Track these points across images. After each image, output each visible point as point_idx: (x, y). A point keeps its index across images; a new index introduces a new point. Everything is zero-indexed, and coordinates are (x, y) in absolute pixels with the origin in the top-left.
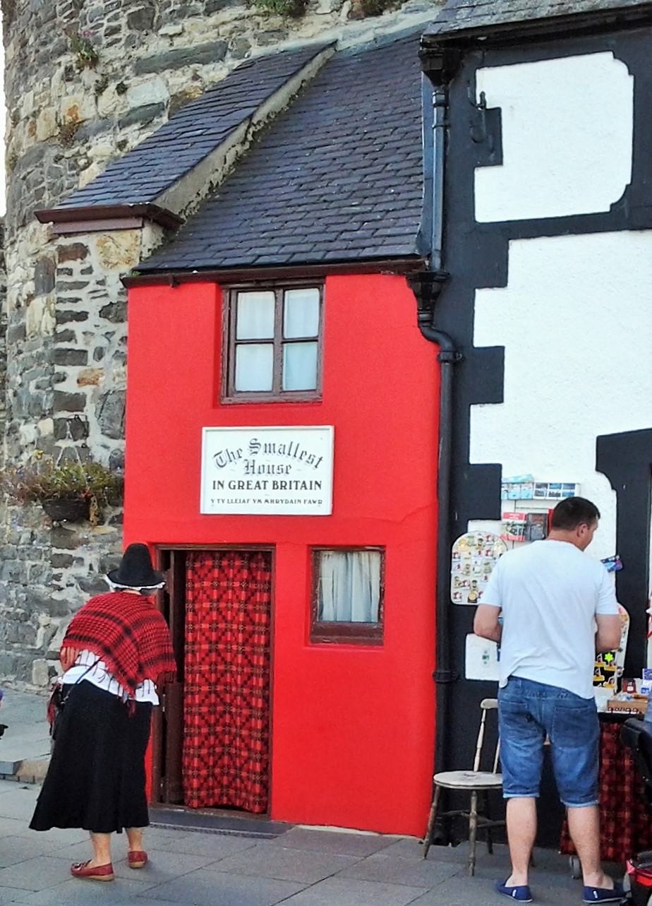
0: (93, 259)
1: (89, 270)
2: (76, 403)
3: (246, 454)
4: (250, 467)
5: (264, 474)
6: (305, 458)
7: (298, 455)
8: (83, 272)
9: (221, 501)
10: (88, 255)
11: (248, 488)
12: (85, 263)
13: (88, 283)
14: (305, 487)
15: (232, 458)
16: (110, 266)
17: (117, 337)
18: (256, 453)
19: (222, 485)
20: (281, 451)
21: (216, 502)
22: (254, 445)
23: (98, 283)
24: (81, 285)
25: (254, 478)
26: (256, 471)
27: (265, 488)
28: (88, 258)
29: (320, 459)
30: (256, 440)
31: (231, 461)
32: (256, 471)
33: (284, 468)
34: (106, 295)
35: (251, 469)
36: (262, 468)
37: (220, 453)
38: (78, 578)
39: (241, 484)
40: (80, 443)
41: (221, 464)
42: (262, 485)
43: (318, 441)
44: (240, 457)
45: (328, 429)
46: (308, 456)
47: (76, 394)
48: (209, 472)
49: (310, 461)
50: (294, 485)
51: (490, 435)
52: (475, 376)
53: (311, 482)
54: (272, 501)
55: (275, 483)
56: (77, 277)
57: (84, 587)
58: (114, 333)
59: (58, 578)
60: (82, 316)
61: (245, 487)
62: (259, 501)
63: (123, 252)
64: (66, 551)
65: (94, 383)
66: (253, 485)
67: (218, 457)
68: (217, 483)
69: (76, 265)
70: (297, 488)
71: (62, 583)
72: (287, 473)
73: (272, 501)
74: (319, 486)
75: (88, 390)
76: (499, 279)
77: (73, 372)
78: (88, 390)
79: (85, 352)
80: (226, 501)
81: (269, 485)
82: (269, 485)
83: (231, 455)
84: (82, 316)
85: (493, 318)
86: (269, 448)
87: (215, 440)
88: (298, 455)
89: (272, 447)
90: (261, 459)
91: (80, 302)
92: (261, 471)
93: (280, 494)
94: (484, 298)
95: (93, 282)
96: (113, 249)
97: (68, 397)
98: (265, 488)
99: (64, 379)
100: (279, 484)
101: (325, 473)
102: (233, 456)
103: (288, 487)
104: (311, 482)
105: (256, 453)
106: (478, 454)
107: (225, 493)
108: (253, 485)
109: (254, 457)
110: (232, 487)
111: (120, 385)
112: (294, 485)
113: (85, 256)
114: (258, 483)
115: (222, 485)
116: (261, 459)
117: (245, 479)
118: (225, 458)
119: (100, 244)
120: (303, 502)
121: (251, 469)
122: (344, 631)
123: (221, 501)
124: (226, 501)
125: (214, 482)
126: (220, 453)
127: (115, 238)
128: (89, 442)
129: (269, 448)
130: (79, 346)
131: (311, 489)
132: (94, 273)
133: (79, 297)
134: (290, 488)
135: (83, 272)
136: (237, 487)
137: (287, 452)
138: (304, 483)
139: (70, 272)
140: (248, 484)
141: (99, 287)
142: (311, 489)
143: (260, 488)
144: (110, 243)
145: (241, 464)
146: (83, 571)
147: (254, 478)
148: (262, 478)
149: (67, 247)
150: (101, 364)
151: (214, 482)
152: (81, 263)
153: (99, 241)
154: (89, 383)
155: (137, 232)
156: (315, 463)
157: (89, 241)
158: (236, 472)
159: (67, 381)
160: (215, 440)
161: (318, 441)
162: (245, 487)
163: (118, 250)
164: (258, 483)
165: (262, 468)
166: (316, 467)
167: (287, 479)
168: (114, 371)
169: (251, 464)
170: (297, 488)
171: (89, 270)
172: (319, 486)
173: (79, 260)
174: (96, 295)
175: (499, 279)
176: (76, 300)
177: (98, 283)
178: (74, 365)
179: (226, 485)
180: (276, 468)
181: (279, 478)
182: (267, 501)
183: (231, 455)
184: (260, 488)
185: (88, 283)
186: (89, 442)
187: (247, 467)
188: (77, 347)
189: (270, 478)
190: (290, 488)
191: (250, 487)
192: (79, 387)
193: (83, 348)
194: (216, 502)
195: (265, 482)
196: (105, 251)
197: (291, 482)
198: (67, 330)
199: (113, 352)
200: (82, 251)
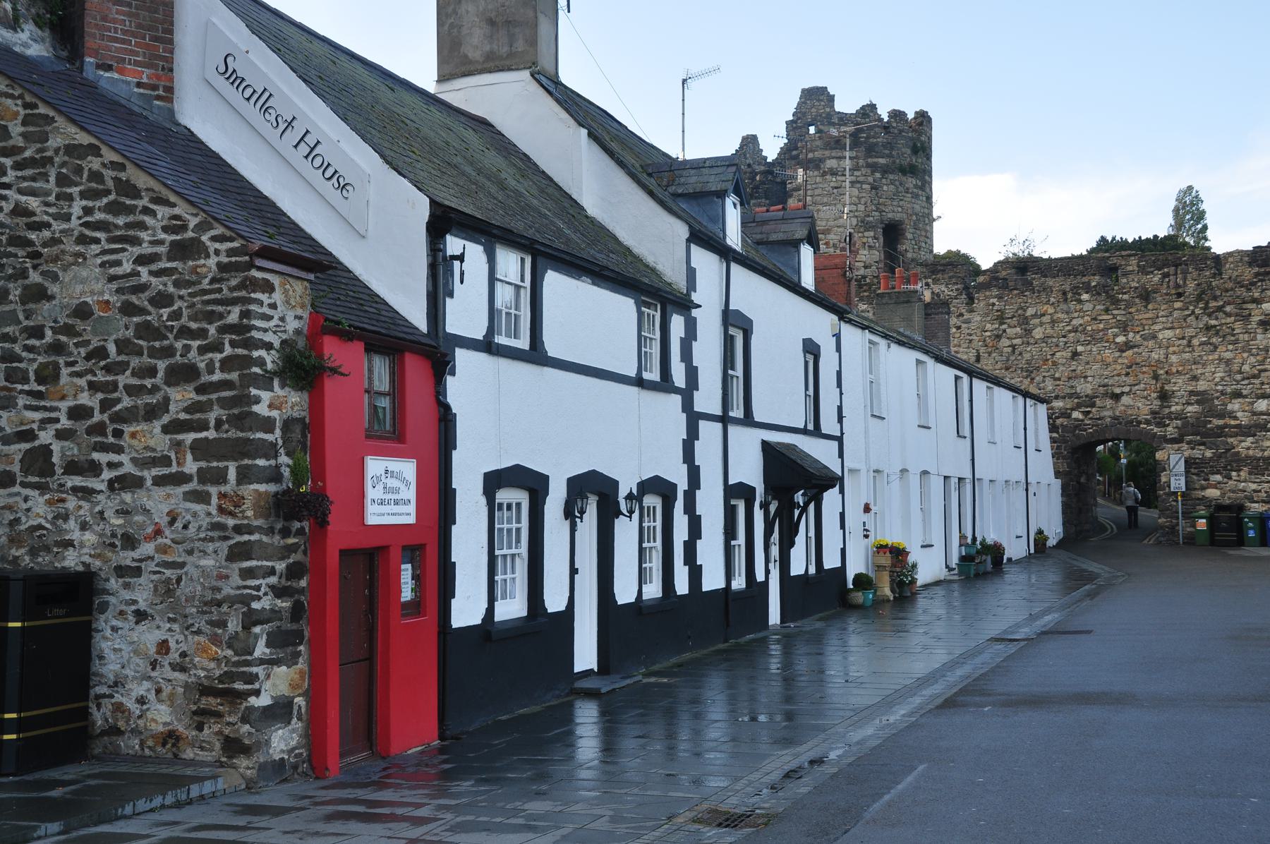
0: (277, 297)
2: (268, 425)
24: (270, 318)
34: (285, 331)
38: (272, 587)
40: (273, 462)
57: (279, 592)
59: (258, 588)
64: (265, 563)
71: (261, 594)
75: (275, 414)
77: (265, 396)
78: (275, 414)
95: (276, 317)
102: (379, 479)
119: (282, 285)
139: (261, 303)
144: (288, 286)
157: (275, 280)
196: (286, 292)
200: (269, 288)
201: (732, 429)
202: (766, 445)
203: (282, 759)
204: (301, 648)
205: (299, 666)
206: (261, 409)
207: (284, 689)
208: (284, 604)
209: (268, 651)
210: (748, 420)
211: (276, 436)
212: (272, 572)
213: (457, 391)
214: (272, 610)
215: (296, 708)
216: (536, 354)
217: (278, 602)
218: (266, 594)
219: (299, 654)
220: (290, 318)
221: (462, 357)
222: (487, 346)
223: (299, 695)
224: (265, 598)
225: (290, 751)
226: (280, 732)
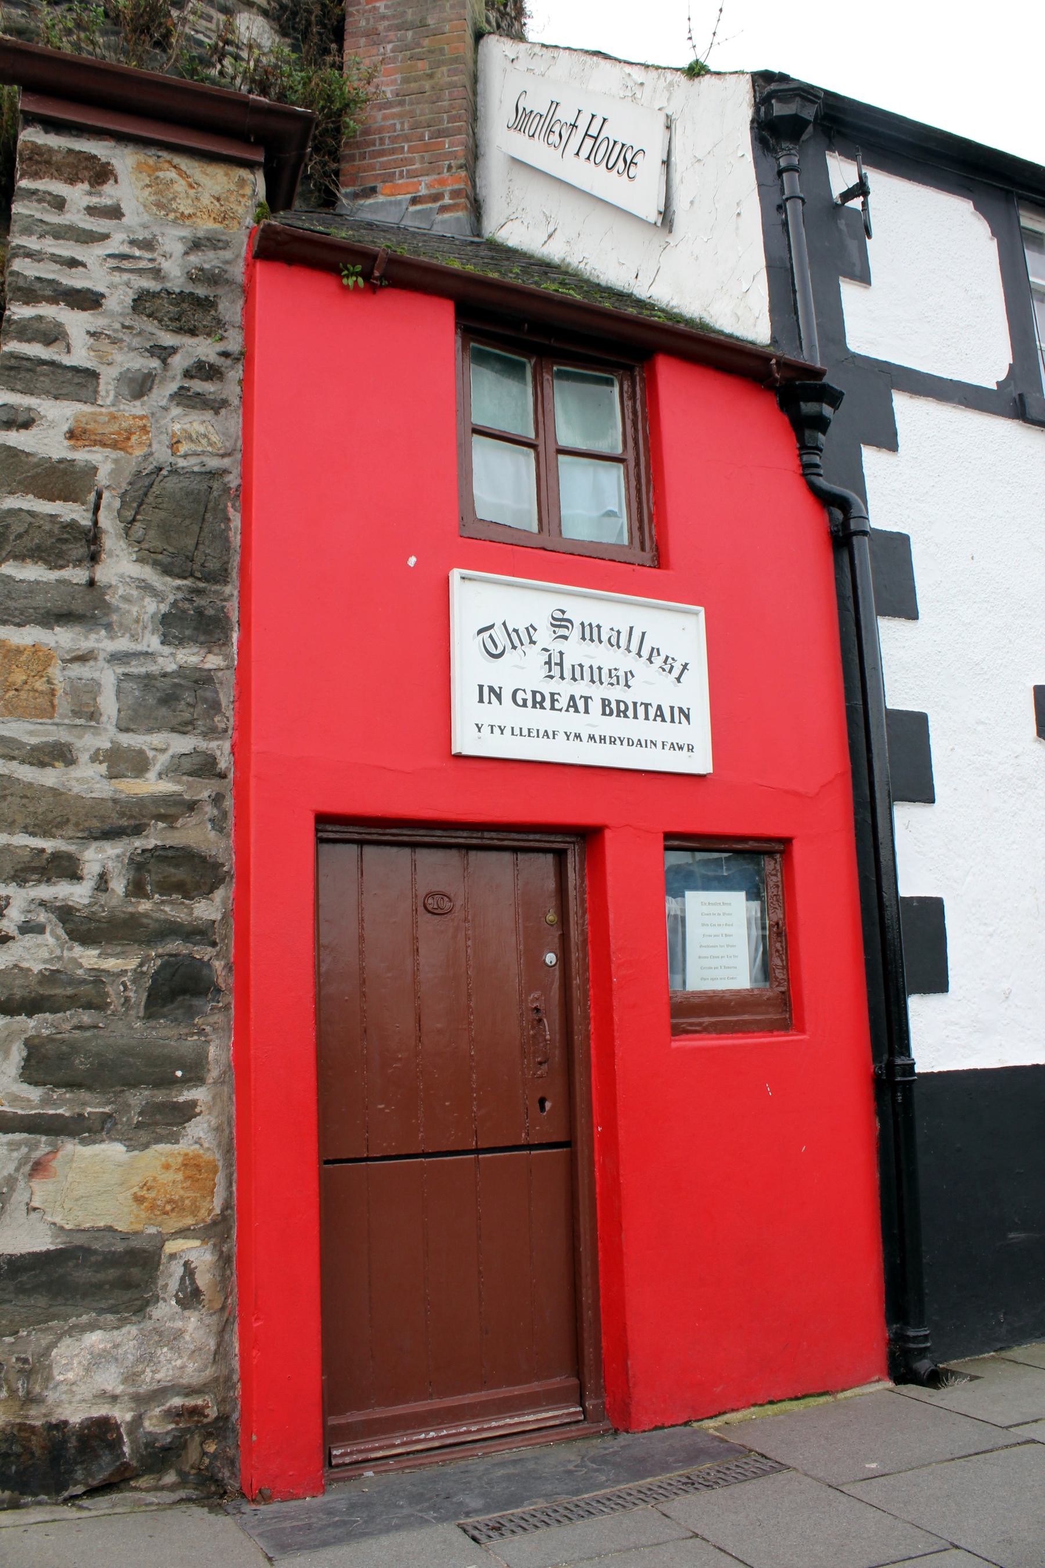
1: (115, 212)
3: (544, 636)
4: (554, 664)
6: (658, 661)
7: (645, 653)
8: (91, 210)
9: (496, 730)
10: (112, 182)
11: (553, 708)
12: (100, 194)
13: (106, 237)
14: (662, 716)
15: (517, 643)
16: (172, 216)
17: (179, 362)
18: (566, 638)
19: (499, 697)
20: (614, 641)
21: (486, 730)
22: (560, 622)
23: (133, 243)
25: (566, 689)
26: (567, 674)
27: (587, 711)
28: (108, 188)
29: (685, 667)
30: (563, 612)
31: (514, 647)
32: (567, 674)
33: (621, 674)
35: (556, 670)
36: (578, 669)
37: (492, 627)
38: (65, 913)
39: (539, 698)
40: (78, 575)
41: (494, 652)
42: (581, 704)
43: (680, 632)
44: (533, 642)
45: (696, 614)
46: (663, 657)
47: (61, 461)
48: (468, 666)
49: (667, 667)
50: (641, 710)
53: (672, 708)
54: (602, 739)
55: (605, 703)
56: (75, 217)
58: (173, 350)
60: (87, 300)
61: (547, 704)
62: (578, 736)
63: (206, 200)
65: (115, 446)
66: (563, 702)
67: (486, 635)
68: (486, 690)
69: (77, 195)
70: (647, 718)
72: (627, 686)
73: (602, 739)
74: (687, 717)
77: (58, 414)
79: (92, 375)
80: (508, 731)
81: (595, 706)
82: (595, 706)
83: (514, 636)
84: (87, 300)
85: (892, 491)
86: (591, 633)
87: (478, 601)
88: (645, 653)
89: (595, 630)
90: (576, 651)
91: (81, 269)
92: (578, 676)
93: (614, 726)
94: (873, 460)
96: (180, 186)
97: (37, 465)
98: (587, 711)
99: (26, 425)
100: (614, 706)
101: (695, 692)
102: (521, 638)
103: (630, 713)
104: (672, 708)
105: (566, 638)
106: (898, 692)
107: (506, 713)
108: (563, 702)
109: (557, 646)
110: (520, 702)
111: (193, 460)
112: (641, 710)
113: (104, 182)
114: (572, 698)
115: (499, 697)
116: (575, 651)
117: (547, 688)
118: (502, 640)
120: (659, 745)
121: (556, 670)
123: (496, 730)
124: (508, 731)
125: (481, 687)
126: (492, 627)
127: (183, 167)
128: (104, 574)
129: (591, 633)
130: (80, 356)
131: (673, 721)
132: (124, 220)
133: (79, 258)
134: (635, 717)
135: (91, 210)
136: (530, 703)
137: (623, 642)
138: (659, 708)
139: (59, 204)
140: (553, 701)
141: (137, 253)
142: (673, 721)
143: (577, 711)
144: (172, 174)
145: (535, 658)
146: (77, 894)
147: (566, 689)
148: (581, 689)
149: (50, 150)
150: (137, 408)
151: (481, 687)
152: (90, 194)
153: (139, 164)
154: (104, 445)
155: (245, 173)
156: (676, 672)
157: (123, 160)
158: (523, 670)
159: (34, 430)
160: (478, 601)
161: (680, 632)
162: (547, 704)
163: (192, 192)
164: (572, 698)
165: (578, 669)
166: (678, 680)
167: (629, 697)
168: (177, 427)
169: (556, 659)
170: (647, 718)
171: (115, 212)
172: (687, 717)
173: (86, 186)
174: (126, 264)
176: (73, 263)
177: (133, 243)
178: (56, 398)
179: (506, 696)
180: (605, 673)
181: (614, 694)
182: (592, 738)
183: (514, 636)
184: (577, 711)
185: (106, 237)
186: (104, 574)
187: (548, 663)
188: (67, 361)
189: (598, 693)
190: (635, 717)
191: (557, 705)
192: (74, 448)
193: (88, 365)
194: (486, 730)
195: (586, 699)
196: (156, 184)
197: (635, 704)
198: (40, 318)
199: (173, 387)
203: (104, 1425)
204: (199, 1094)
205: (184, 1146)
208: (119, 963)
209: (35, 1094)
212: (64, 867)
214: (51, 977)
215: (172, 1277)
217: (88, 957)
218: (28, 928)
219: (186, 1112)
223: (183, 1233)
224: (29, 940)
225: (142, 1401)
226: (95, 1339)
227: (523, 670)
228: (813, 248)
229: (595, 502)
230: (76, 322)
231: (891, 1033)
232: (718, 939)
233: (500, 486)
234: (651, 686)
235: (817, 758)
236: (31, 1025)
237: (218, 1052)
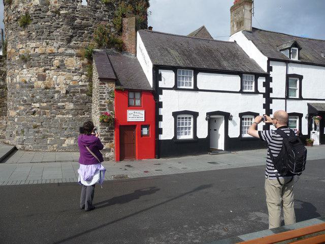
2: (104, 106)
5: (135, 116)
22: (134, 112)
43: (143, 112)
48: (128, 116)
51: (162, 111)
52: (160, 105)
57: (107, 132)
69: (103, 85)
76: (162, 94)
122: (145, 135)
158: (132, 116)
175: (162, 94)
201: (287, 101)
202: (308, 104)
206: (103, 103)
207: (109, 147)
210: (301, 98)
211: (107, 107)
213: (162, 98)
216: (196, 89)
220: (109, 88)
221: (164, 91)
222: (176, 88)
227: (132, 116)
228: (157, 77)
229: (138, 102)
230: (104, 95)
231: (158, 137)
232: (145, 131)
233: (132, 102)
234: (140, 116)
235: (152, 119)
236: (104, 137)
237: (114, 138)
